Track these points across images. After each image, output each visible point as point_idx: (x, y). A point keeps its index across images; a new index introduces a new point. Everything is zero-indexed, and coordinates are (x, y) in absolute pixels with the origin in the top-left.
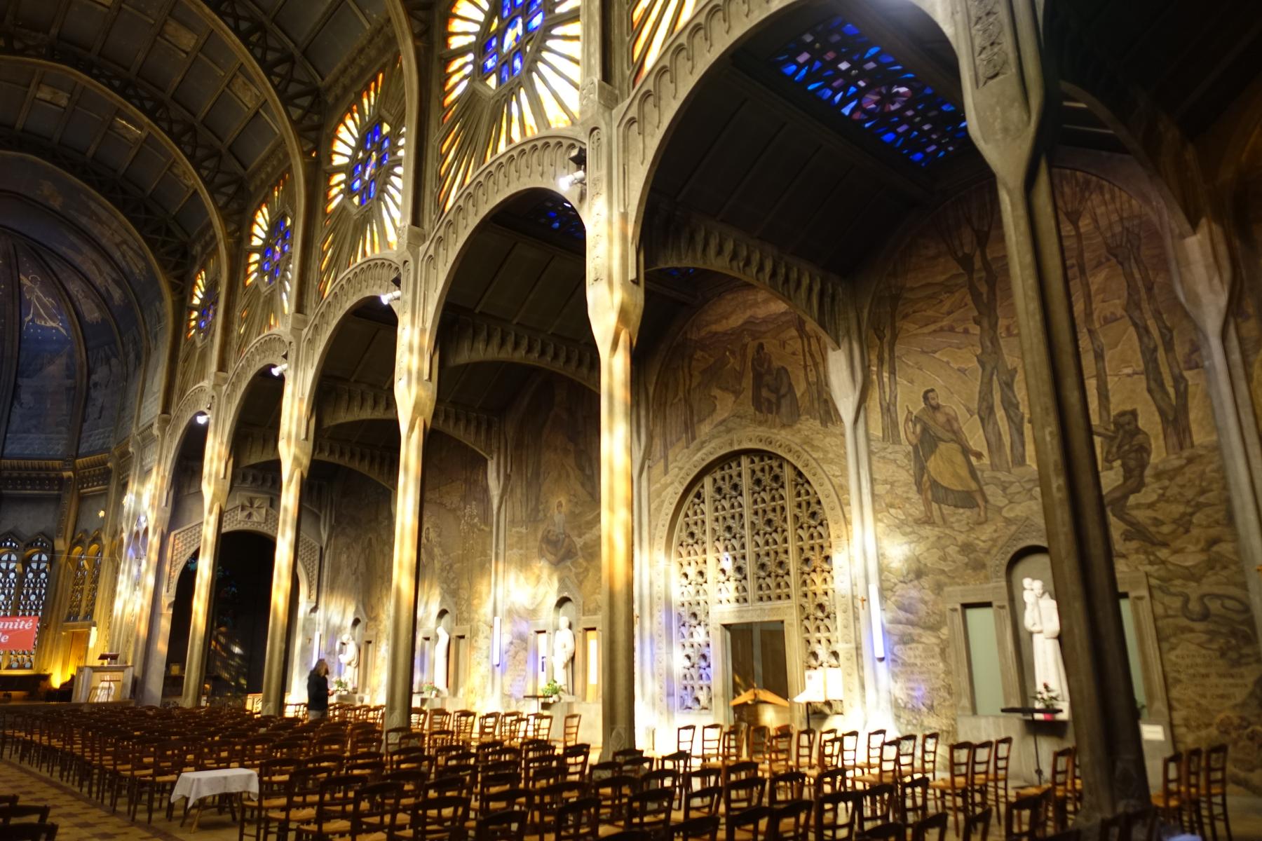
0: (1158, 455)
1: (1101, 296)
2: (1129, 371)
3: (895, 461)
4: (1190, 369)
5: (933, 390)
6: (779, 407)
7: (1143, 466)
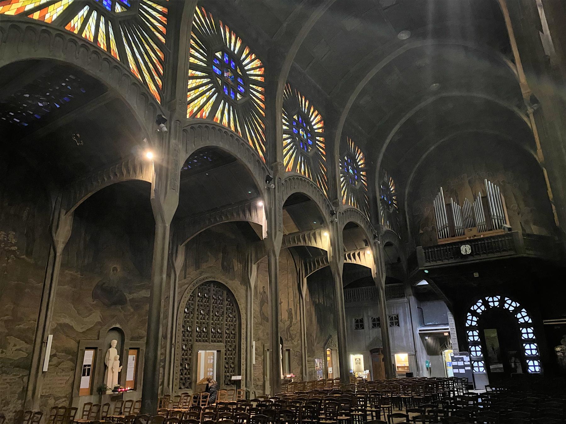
6: (229, 272)
7: (292, 322)
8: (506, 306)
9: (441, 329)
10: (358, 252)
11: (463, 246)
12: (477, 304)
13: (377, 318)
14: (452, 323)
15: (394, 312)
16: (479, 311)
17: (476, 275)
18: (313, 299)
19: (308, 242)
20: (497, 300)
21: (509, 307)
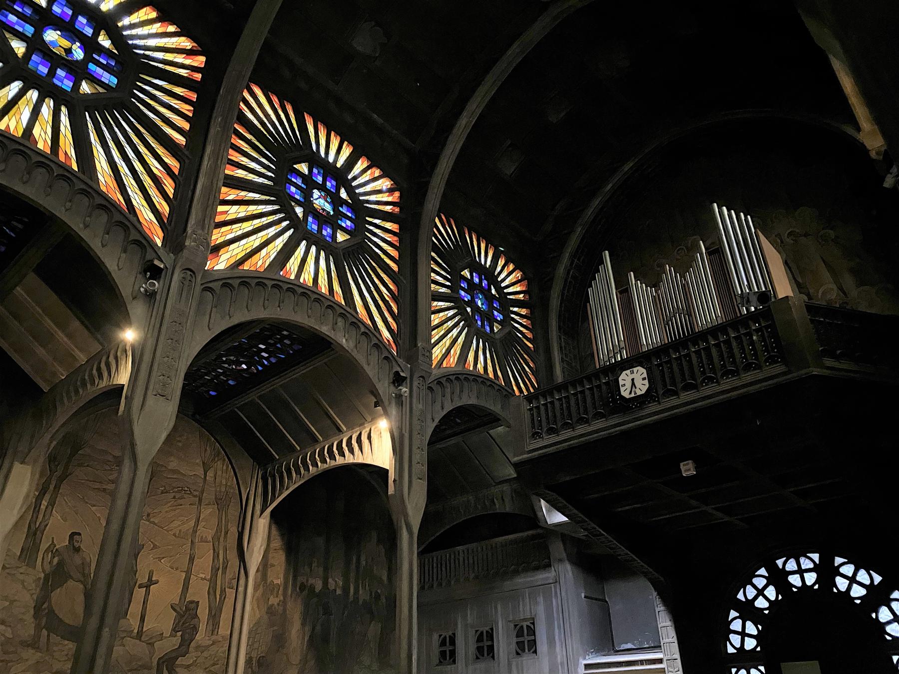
0: (201, 636)
1: (204, 523)
2: (203, 576)
3: (23, 582)
4: (229, 588)
5: (79, 534)
8: (842, 584)
9: (642, 662)
10: (368, 429)
11: (624, 373)
12: (756, 581)
13: (487, 632)
14: (671, 640)
15: (524, 611)
16: (761, 603)
17: (688, 469)
18: (300, 579)
19: (114, 374)
20: (811, 566)
21: (849, 588)
